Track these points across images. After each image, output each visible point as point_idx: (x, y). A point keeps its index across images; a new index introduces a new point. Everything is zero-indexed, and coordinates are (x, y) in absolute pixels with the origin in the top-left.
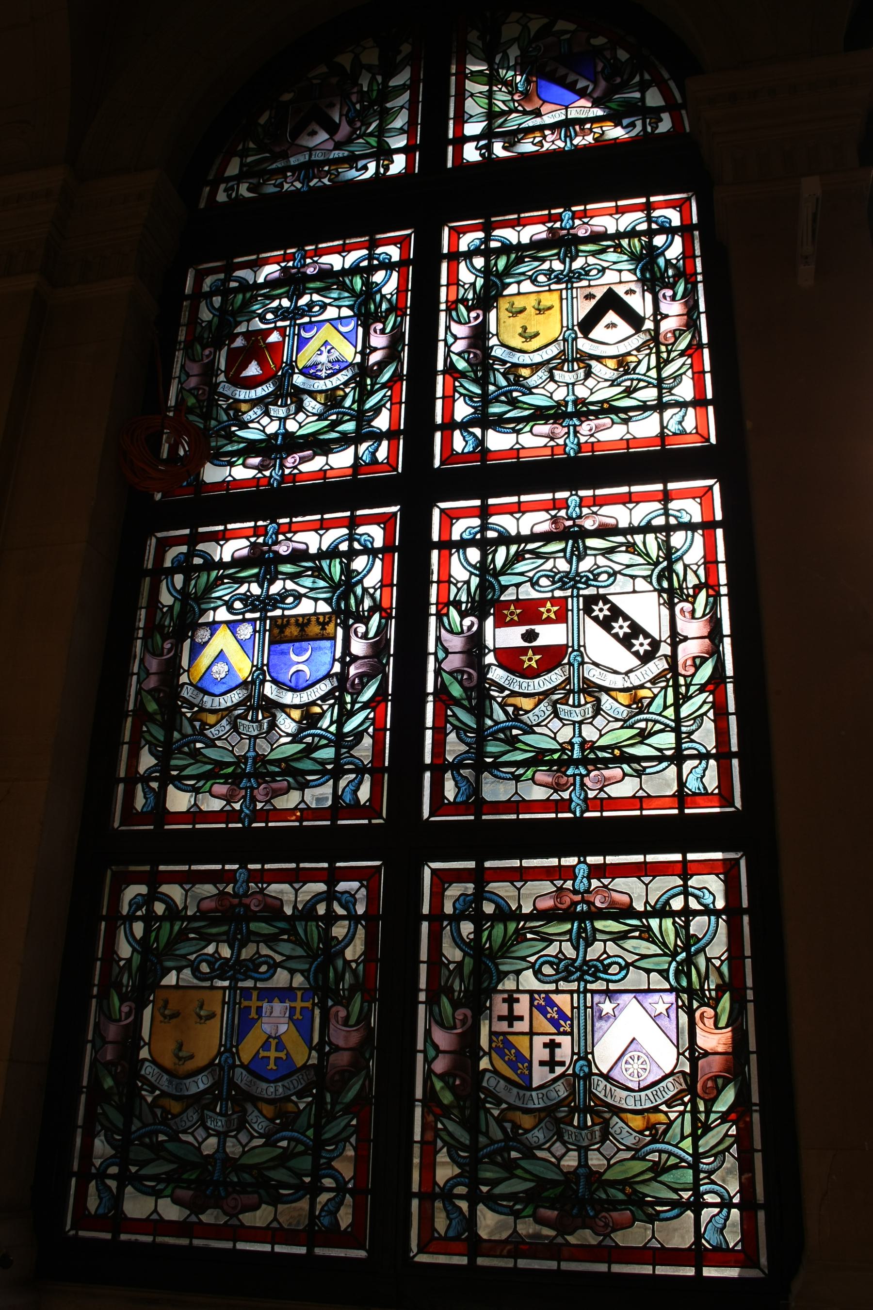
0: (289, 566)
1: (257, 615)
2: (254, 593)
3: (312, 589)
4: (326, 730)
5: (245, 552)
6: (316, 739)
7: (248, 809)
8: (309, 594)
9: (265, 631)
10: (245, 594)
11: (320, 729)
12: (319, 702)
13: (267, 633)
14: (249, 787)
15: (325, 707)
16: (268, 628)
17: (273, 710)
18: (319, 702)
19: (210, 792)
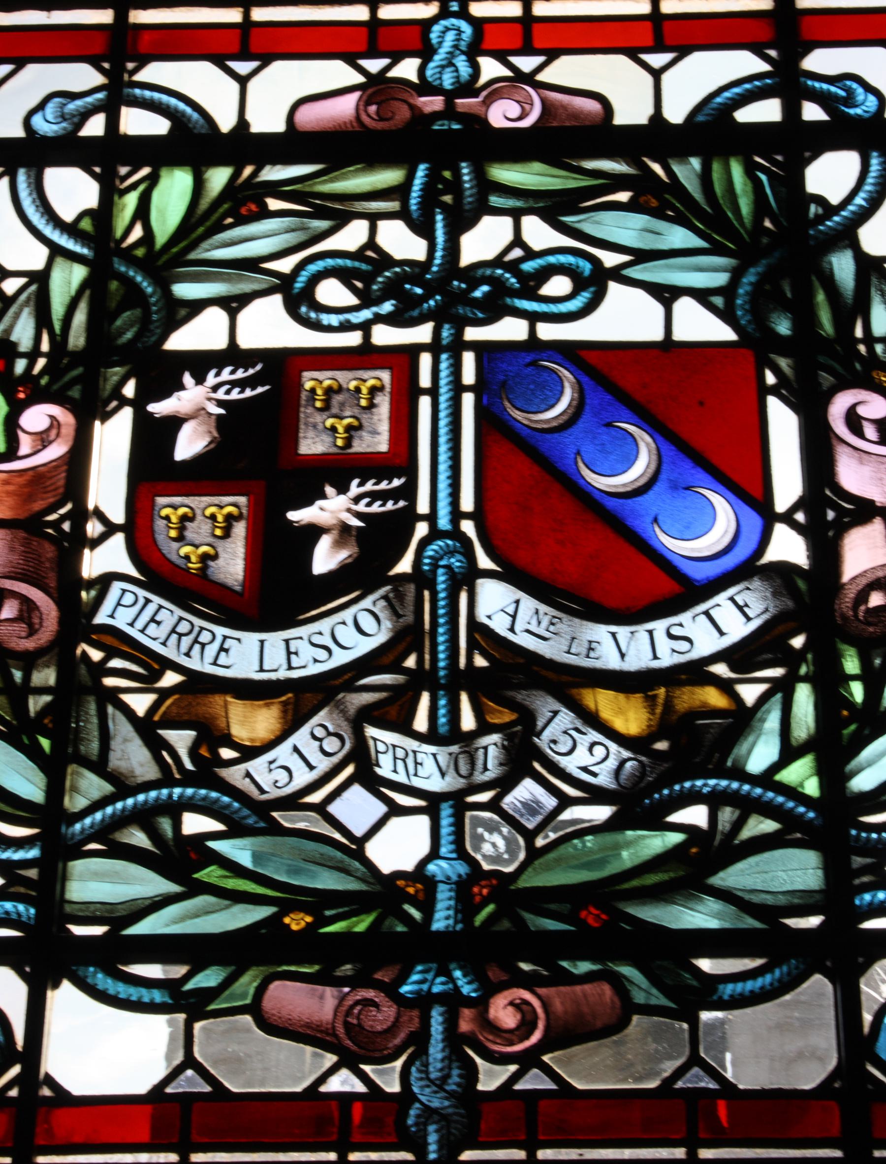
0: (537, 166)
1: (423, 333)
2: (398, 254)
3: (642, 256)
4: (767, 779)
5: (346, 106)
6: (727, 815)
7: (440, 1084)
8: (634, 273)
9: (458, 388)
10: (358, 255)
11: (740, 774)
12: (721, 669)
13: (468, 400)
14: (440, 998)
15: (750, 693)
16: (469, 376)
17: (521, 696)
18: (721, 669)
19: (255, 1009)
